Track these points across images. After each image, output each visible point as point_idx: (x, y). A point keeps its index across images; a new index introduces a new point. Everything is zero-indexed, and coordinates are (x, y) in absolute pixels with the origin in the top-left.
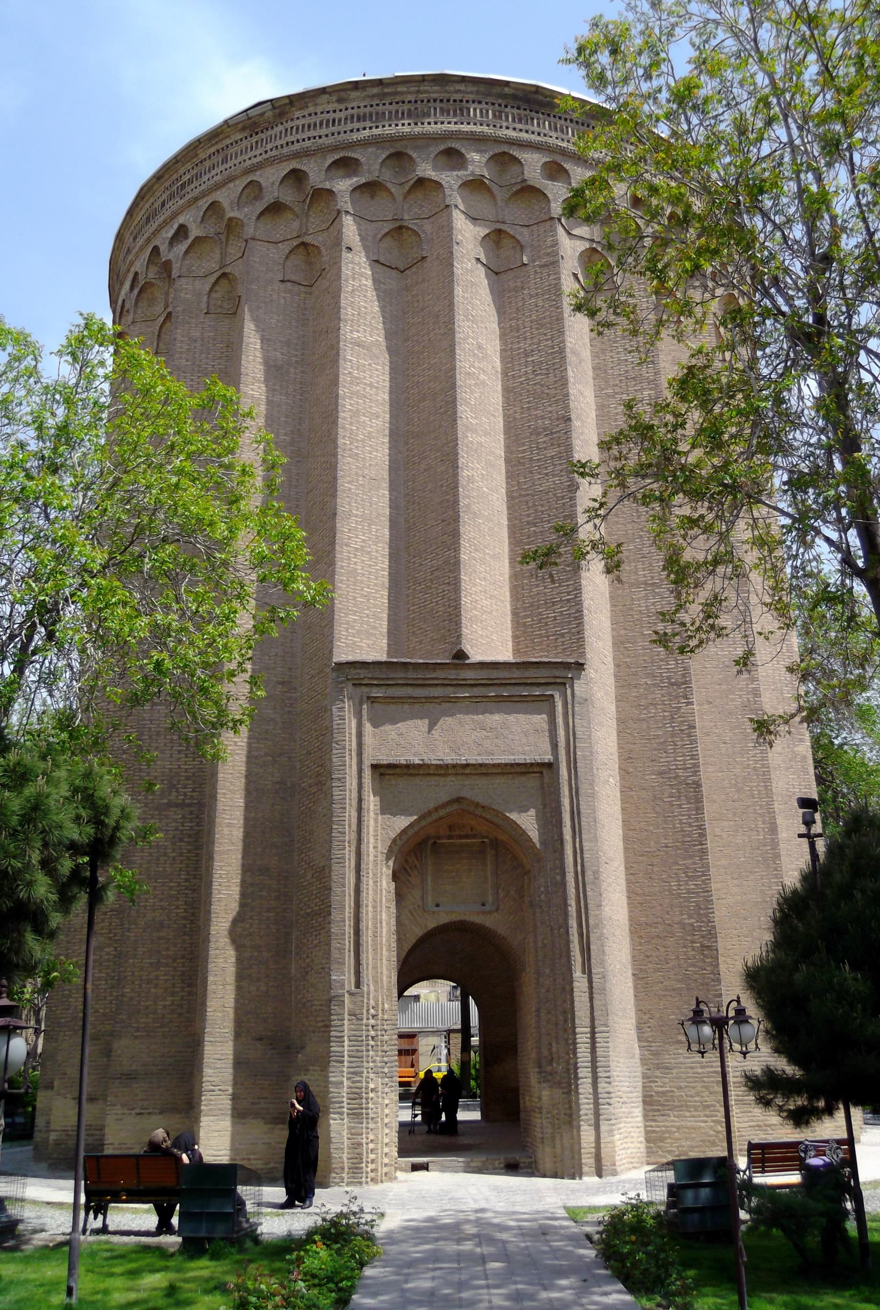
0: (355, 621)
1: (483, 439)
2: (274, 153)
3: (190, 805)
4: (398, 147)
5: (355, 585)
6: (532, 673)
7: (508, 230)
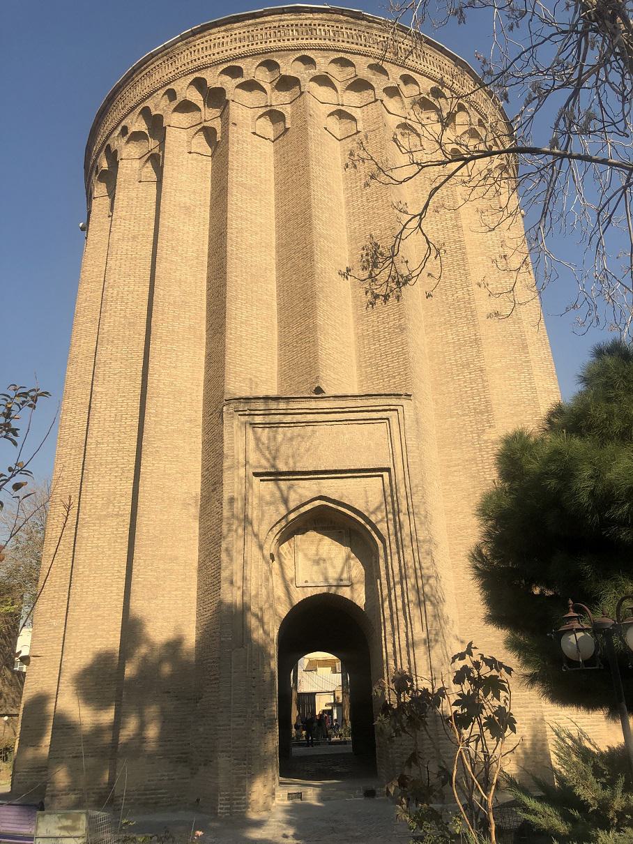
0: (241, 372)
1: (332, 245)
2: (184, 68)
3: (122, 516)
4: (267, 57)
5: (241, 346)
6: (371, 402)
7: (346, 110)
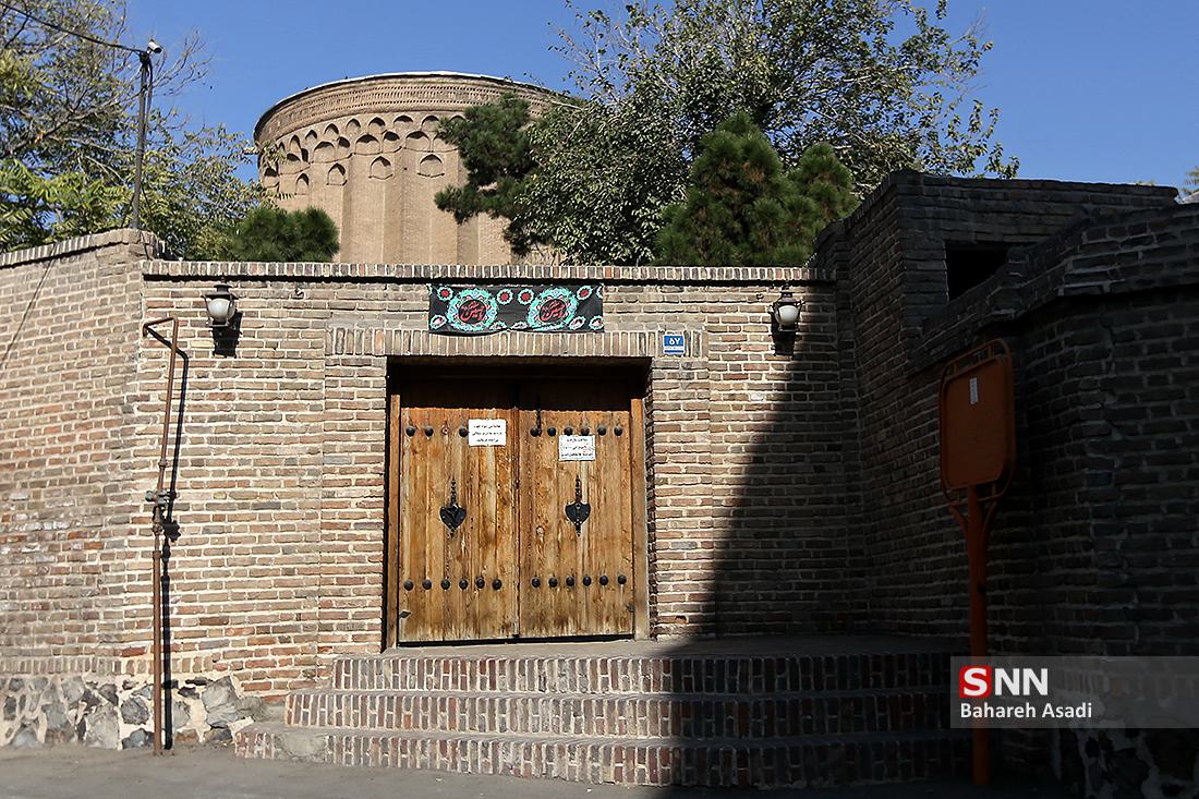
4: (431, 113)
